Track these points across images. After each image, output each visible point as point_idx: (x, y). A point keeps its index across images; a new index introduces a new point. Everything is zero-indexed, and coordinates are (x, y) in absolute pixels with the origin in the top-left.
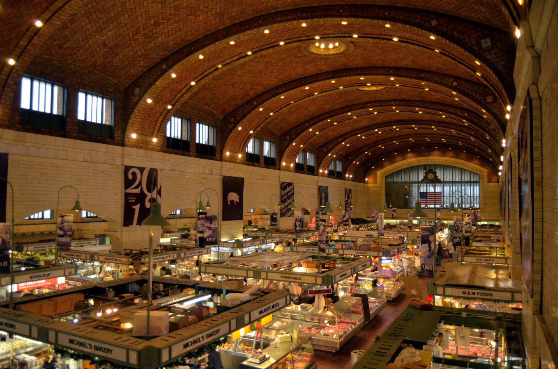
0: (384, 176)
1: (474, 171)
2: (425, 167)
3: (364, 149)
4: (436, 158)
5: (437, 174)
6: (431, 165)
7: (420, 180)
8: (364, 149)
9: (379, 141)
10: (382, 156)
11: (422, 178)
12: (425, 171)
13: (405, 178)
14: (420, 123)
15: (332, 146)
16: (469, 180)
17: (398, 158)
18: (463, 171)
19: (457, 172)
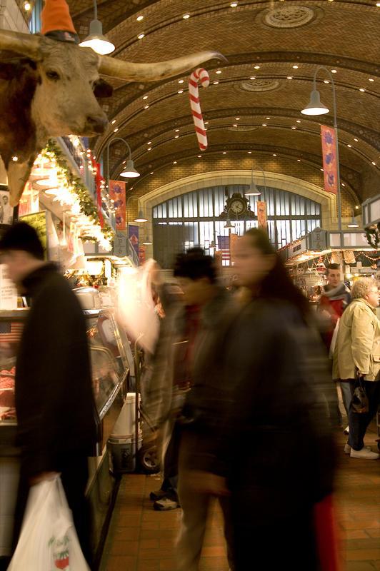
0: (151, 207)
1: (313, 198)
2: (226, 190)
3: (146, 135)
4: (246, 173)
5: (248, 203)
6: (234, 186)
7: (217, 215)
8: (146, 135)
9: (178, 119)
10: (150, 166)
11: (222, 210)
12: (226, 199)
13: (190, 211)
14: (313, 60)
15: (122, 101)
16: (303, 213)
17: (178, 171)
18: (293, 199)
19: (282, 200)
